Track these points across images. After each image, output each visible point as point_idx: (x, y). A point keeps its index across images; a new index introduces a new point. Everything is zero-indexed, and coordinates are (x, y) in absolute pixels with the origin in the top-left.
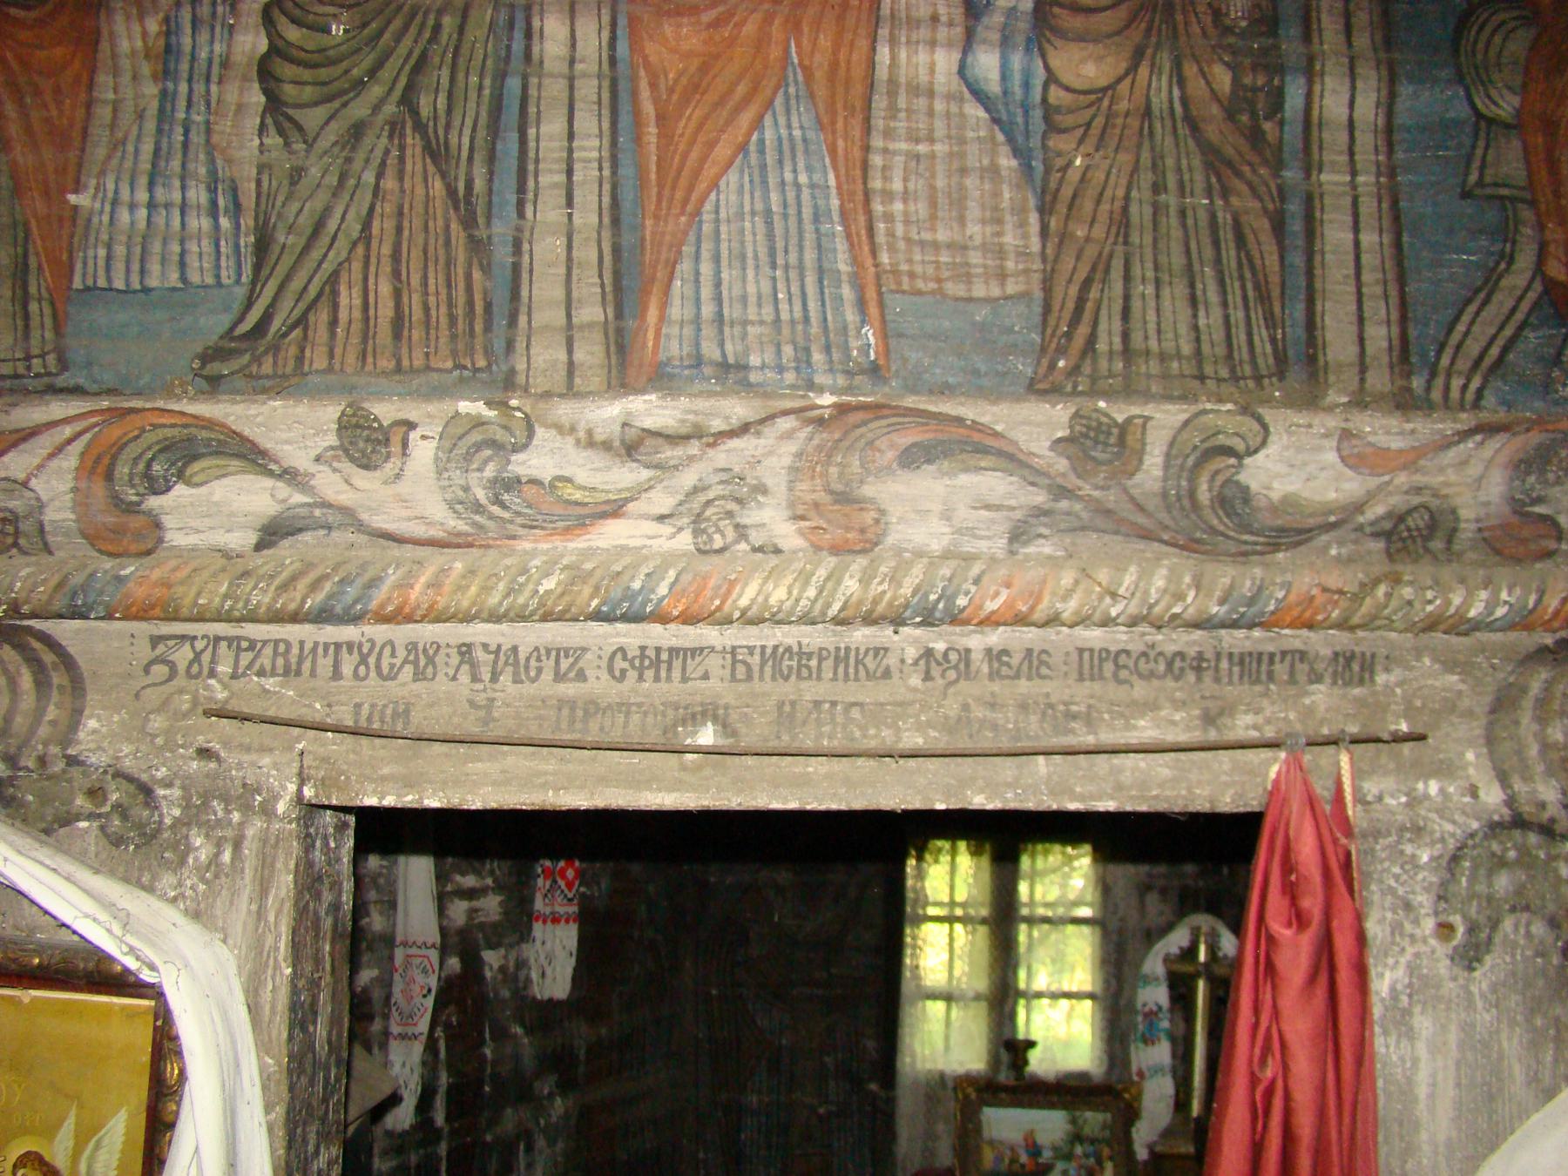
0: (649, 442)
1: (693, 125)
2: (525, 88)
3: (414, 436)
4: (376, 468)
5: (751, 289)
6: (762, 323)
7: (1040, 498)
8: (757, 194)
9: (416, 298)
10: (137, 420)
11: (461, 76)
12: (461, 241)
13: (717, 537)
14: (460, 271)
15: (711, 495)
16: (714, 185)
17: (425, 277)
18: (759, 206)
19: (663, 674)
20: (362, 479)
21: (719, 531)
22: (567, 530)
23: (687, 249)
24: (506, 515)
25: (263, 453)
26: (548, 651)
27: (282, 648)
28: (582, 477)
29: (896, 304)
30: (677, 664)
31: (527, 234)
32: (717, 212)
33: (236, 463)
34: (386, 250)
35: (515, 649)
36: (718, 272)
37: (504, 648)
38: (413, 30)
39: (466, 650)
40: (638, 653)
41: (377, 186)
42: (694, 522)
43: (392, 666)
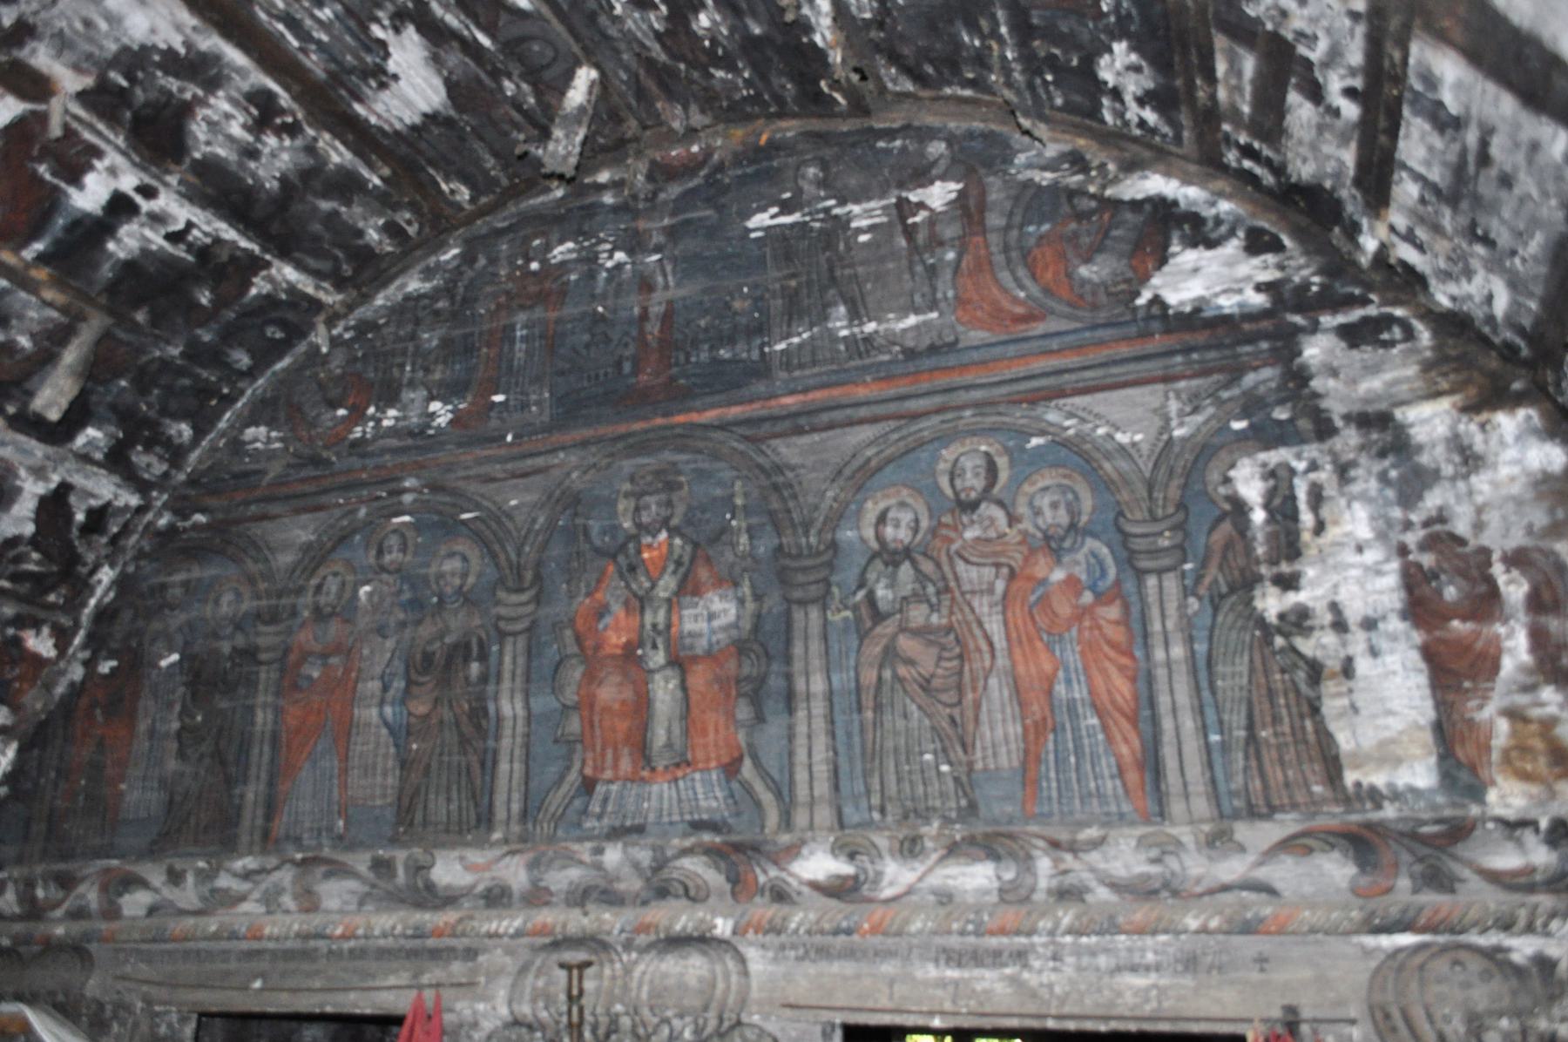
7: (366, 889)
20: (176, 891)
29: (350, 812)
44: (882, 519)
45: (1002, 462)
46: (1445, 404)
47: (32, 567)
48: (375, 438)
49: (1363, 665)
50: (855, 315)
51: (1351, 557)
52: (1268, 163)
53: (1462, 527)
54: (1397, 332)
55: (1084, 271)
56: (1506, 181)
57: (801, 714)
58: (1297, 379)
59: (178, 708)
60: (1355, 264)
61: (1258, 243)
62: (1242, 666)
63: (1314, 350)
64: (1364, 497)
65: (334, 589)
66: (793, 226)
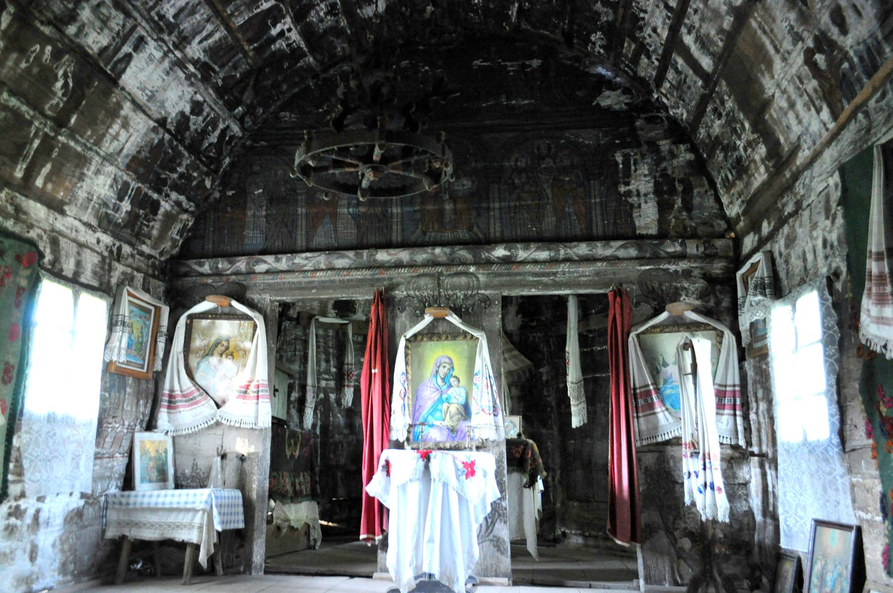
44: (517, 160)
45: (553, 146)
46: (668, 141)
47: (212, 154)
49: (643, 206)
50: (509, 98)
51: (643, 178)
52: (632, 70)
53: (669, 172)
54: (659, 121)
55: (578, 93)
56: (689, 88)
57: (492, 213)
58: (634, 129)
59: (264, 208)
60: (650, 101)
61: (626, 91)
62: (614, 204)
63: (638, 123)
64: (647, 163)
66: (487, 66)
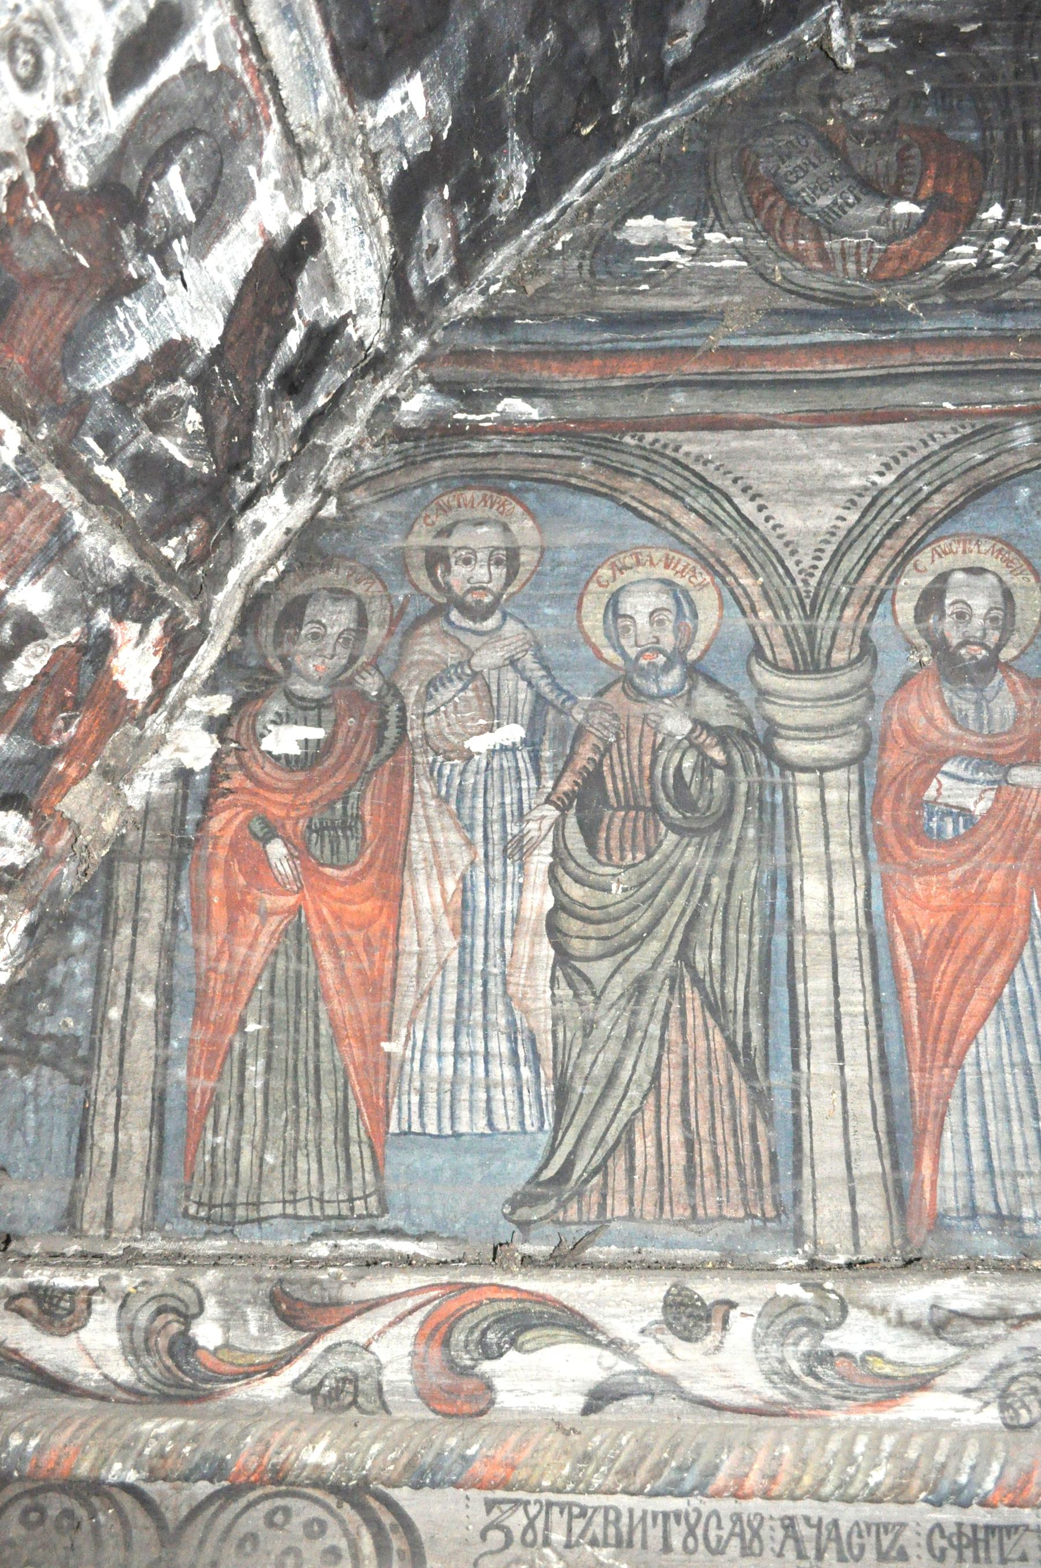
0: (956, 1322)
1: (948, 979)
2: (791, 944)
3: (734, 1314)
4: (697, 1340)
5: (1018, 1141)
6: (1030, 1174)
8: (1015, 1046)
9: (706, 1147)
10: (473, 1296)
11: (732, 933)
12: (744, 1094)
13: (1023, 1412)
14: (746, 1124)
15: (1016, 1371)
16: (973, 1037)
17: (713, 1128)
18: (1017, 1058)
19: (982, 1555)
20: (682, 1348)
21: (1024, 1406)
22: (877, 1403)
23: (954, 1103)
24: (819, 1386)
25: (592, 1326)
26: (868, 1527)
27: (612, 1516)
28: (891, 1354)
30: (994, 1542)
31: (804, 1087)
32: (978, 1064)
33: (564, 1333)
34: (675, 1099)
35: (835, 1523)
36: (985, 1125)
37: (825, 1522)
38: (686, 889)
39: (789, 1524)
40: (954, 1530)
41: (662, 1039)
42: (1000, 1397)
43: (719, 1539)
48: (1016, 278)
59: (541, 860)
65: (980, 604)
